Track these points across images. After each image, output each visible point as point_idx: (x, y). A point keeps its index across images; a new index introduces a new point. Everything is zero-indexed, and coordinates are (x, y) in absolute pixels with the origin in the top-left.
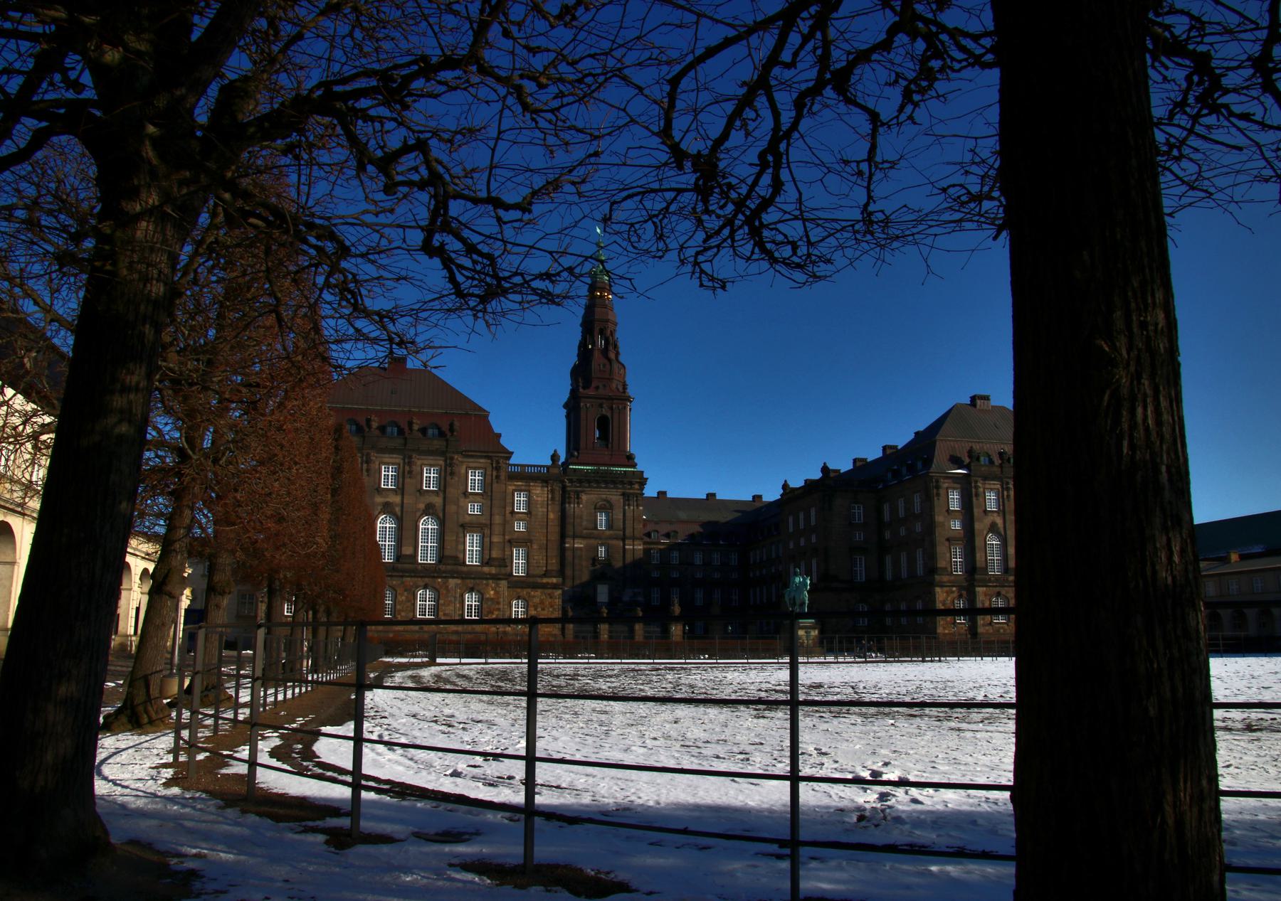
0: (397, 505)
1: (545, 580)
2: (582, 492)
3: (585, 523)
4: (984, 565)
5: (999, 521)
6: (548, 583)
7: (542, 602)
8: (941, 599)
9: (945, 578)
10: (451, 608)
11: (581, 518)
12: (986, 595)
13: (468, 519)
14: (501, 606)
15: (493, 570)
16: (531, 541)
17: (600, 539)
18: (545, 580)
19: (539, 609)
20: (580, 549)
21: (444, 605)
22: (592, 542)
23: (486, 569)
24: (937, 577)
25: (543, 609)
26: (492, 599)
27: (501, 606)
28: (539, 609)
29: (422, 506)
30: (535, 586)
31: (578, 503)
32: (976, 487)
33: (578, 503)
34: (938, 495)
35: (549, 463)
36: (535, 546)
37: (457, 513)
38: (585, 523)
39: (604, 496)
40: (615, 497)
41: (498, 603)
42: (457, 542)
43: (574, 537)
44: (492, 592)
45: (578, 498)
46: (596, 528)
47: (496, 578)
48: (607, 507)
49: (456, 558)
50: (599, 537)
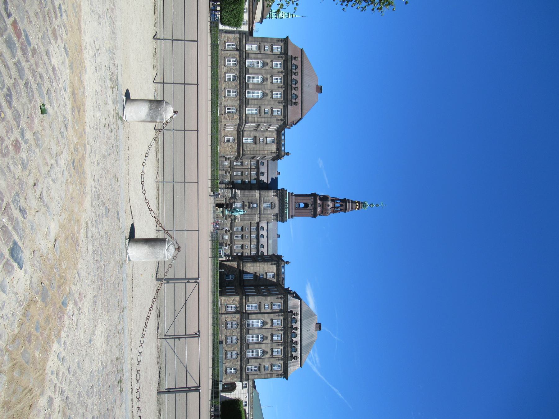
0: (267, 83)
1: (241, 149)
2: (278, 197)
3: (266, 198)
4: (250, 318)
5: (268, 326)
6: (240, 150)
7: (233, 148)
8: (236, 298)
9: (244, 300)
10: (230, 102)
11: (268, 197)
12: (238, 318)
13: (263, 109)
14: (231, 121)
15: (244, 118)
16: (256, 144)
17: (259, 205)
18: (241, 149)
19: (231, 147)
20: (255, 197)
21: (231, 99)
22: (258, 202)
23: (244, 115)
24: (244, 297)
25: (230, 149)
26: (233, 117)
27: (231, 121)
28: (231, 147)
29: (267, 91)
30: (239, 146)
31: (273, 195)
32: (282, 315)
33: (273, 195)
34: (278, 298)
35: (286, 152)
36: (254, 146)
37: (265, 105)
38: (266, 198)
39: (276, 206)
40: (275, 211)
41: (232, 119)
42: (254, 104)
43: (260, 194)
44: (236, 117)
45: (275, 195)
46: (264, 203)
47: (241, 119)
48: (272, 206)
49: (248, 104)
50: (259, 206)
